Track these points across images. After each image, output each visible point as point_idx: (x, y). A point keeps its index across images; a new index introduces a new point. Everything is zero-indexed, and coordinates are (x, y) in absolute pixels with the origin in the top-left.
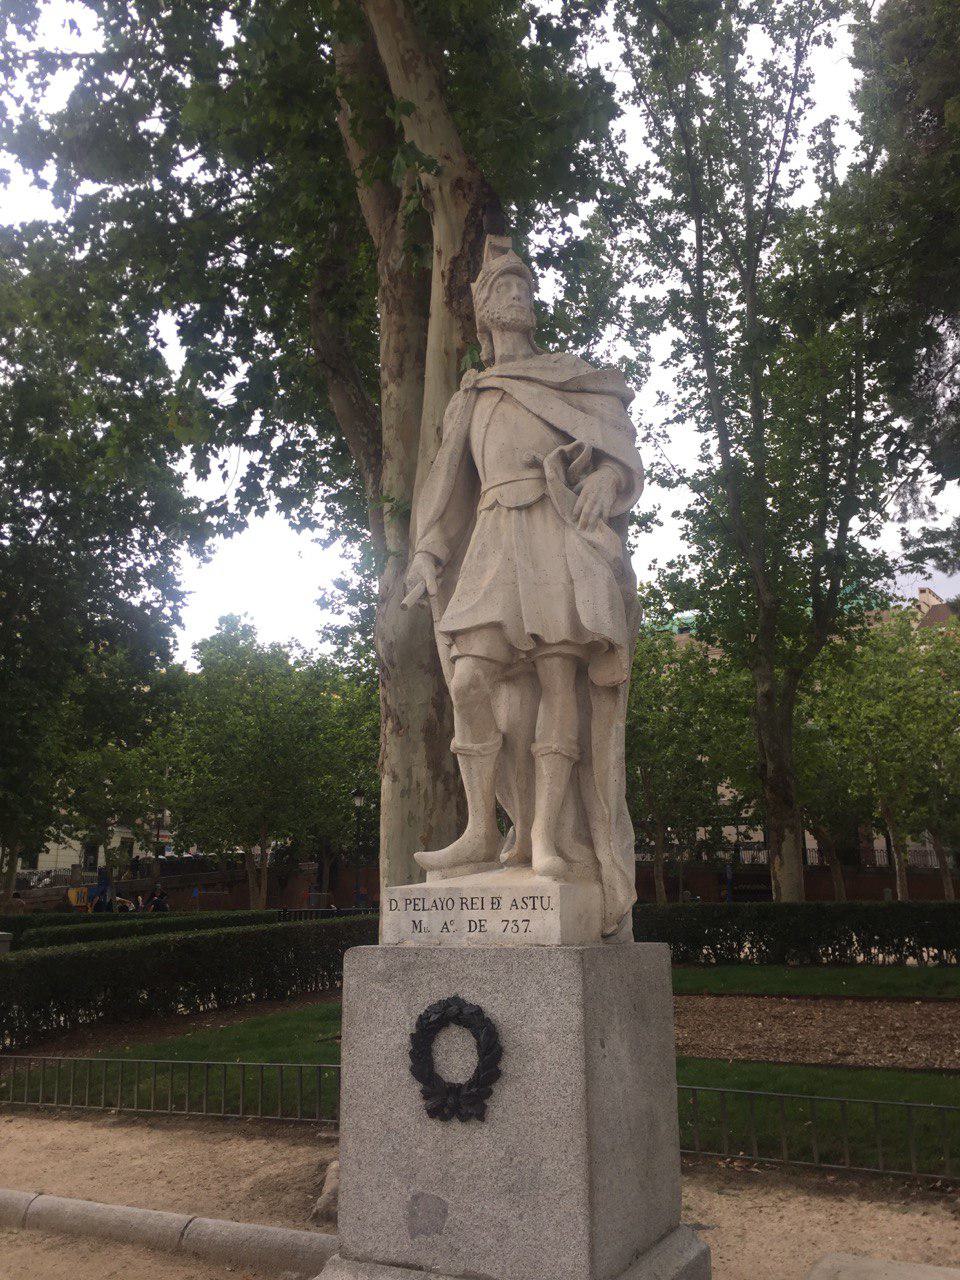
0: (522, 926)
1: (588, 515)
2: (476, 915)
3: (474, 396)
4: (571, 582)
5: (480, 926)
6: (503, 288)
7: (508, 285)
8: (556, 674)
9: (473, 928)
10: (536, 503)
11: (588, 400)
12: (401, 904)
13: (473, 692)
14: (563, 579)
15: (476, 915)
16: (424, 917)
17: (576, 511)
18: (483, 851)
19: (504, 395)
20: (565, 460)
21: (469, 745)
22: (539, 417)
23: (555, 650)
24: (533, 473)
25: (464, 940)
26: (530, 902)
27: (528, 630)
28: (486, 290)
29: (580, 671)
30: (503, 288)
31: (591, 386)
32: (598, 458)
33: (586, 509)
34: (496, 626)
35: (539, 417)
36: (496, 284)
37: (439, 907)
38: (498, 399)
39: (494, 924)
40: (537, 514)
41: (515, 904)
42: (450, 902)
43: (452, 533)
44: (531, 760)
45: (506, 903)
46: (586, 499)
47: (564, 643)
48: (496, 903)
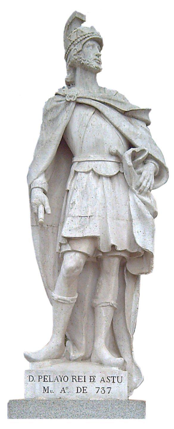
0: (107, 390)
1: (144, 188)
2: (81, 385)
3: (74, 106)
4: (131, 220)
5: (84, 390)
6: (91, 48)
7: (93, 46)
8: (112, 266)
9: (79, 391)
10: (115, 175)
11: (134, 121)
12: (36, 378)
13: (77, 271)
14: (127, 216)
15: (81, 385)
16: (50, 385)
17: (138, 184)
18: (57, 354)
19: (97, 111)
20: (134, 156)
21: (65, 298)
22: (117, 129)
23: (119, 254)
24: (113, 159)
25: (74, 396)
26: (111, 379)
27: (113, 242)
28: (81, 46)
29: (123, 265)
30: (91, 48)
31: (138, 116)
32: (150, 157)
33: (144, 184)
34: (94, 239)
35: (117, 129)
36: (87, 44)
37: (59, 380)
38: (93, 113)
39: (91, 388)
40: (115, 179)
41: (103, 380)
42: (66, 378)
43: (49, 178)
44: (93, 309)
45: (98, 379)
46: (144, 178)
47: (125, 251)
48: (92, 379)
